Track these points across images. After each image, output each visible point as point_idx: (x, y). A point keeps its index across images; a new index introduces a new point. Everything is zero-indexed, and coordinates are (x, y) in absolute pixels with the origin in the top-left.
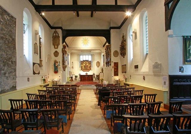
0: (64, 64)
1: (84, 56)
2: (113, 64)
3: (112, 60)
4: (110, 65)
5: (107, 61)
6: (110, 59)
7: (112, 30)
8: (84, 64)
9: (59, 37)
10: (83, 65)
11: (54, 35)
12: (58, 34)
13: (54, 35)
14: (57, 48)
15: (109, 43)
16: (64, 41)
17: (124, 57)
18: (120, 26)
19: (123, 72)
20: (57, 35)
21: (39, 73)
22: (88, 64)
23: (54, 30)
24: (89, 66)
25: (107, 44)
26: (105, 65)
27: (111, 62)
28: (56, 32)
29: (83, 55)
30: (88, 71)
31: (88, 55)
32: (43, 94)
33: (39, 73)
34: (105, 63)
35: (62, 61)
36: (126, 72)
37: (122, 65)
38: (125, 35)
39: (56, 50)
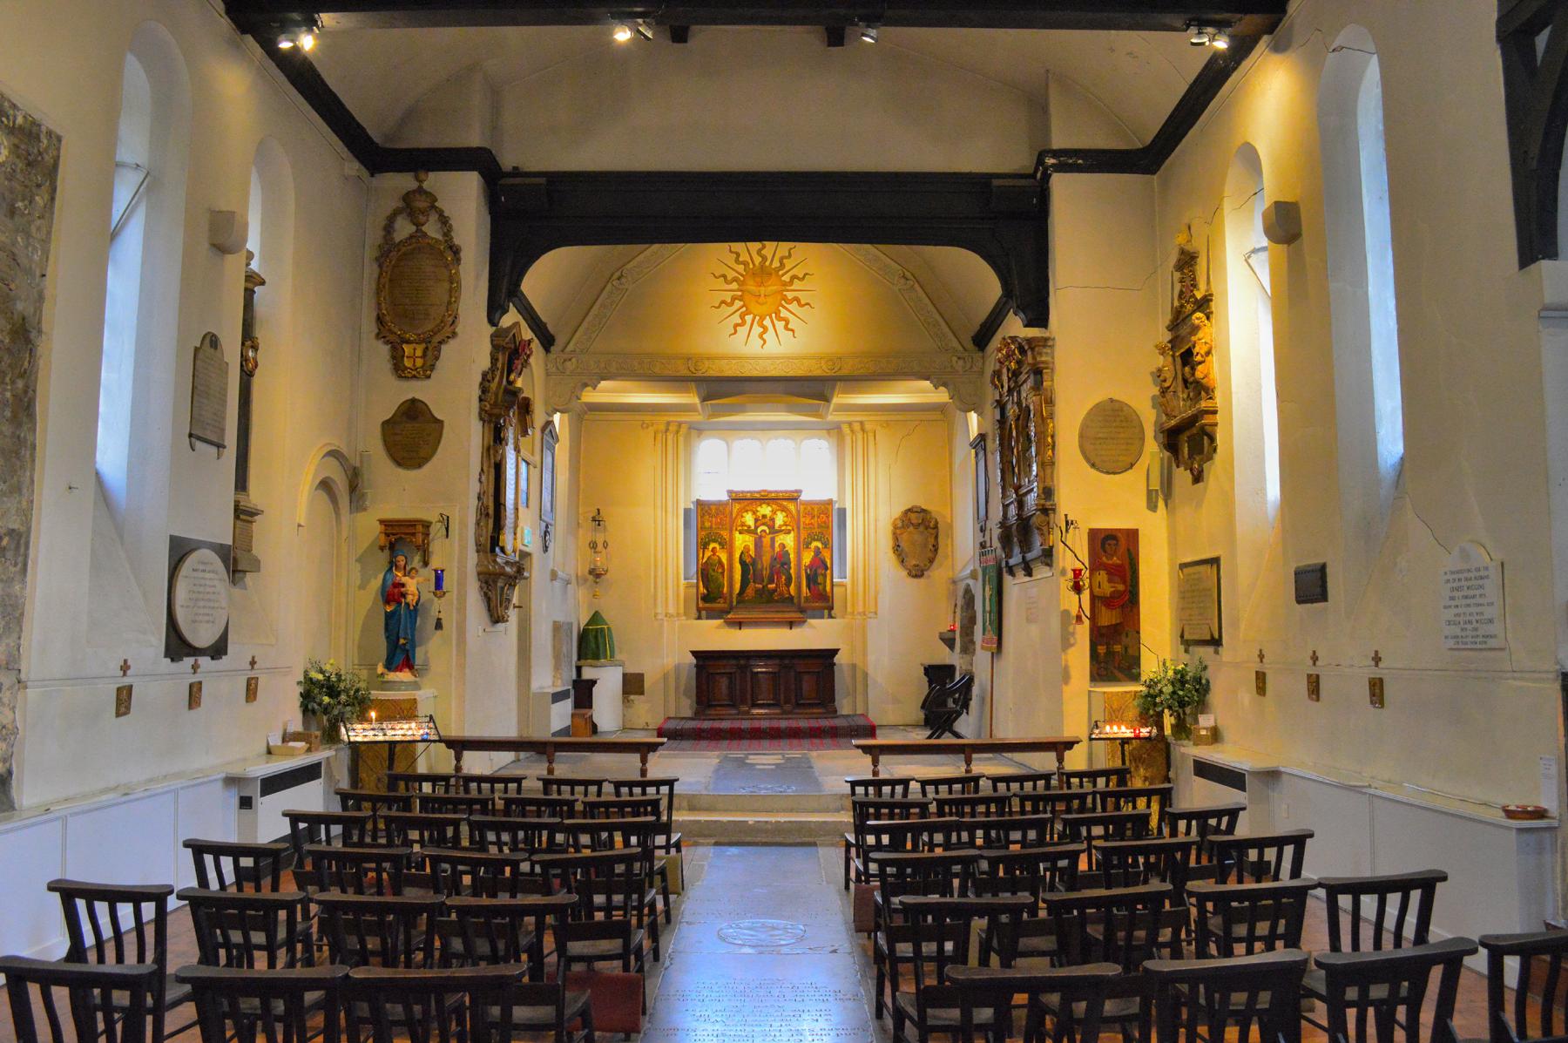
0: (495, 541)
2: (1073, 553)
3: (1068, 502)
4: (1048, 556)
5: (1013, 510)
6: (1048, 493)
7: (1064, 188)
9: (456, 251)
10: (728, 545)
11: (404, 229)
12: (444, 221)
13: (404, 229)
14: (426, 371)
15: (1038, 314)
16: (504, 291)
18: (1148, 139)
20: (432, 229)
22: (789, 541)
23: (403, 182)
24: (807, 558)
25: (1015, 326)
27: (1046, 529)
28: (416, 206)
30: (791, 624)
35: (482, 513)
37: (1183, 566)
38: (1198, 244)
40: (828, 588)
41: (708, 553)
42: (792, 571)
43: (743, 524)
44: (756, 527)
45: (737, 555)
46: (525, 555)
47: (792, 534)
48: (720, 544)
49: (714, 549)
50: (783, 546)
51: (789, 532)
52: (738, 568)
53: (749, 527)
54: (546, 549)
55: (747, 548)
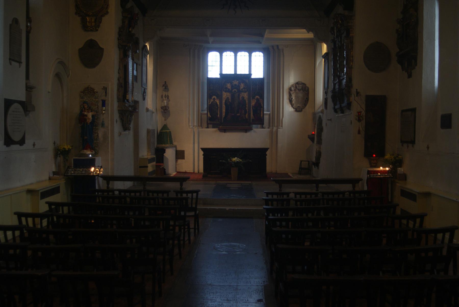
1: (228, 56)
8: (225, 95)
10: (220, 97)
17: (410, 76)
19: (403, 142)
21: (22, 142)
22: (245, 95)
24: (253, 103)
26: (330, 104)
29: (221, 51)
31: (250, 51)
32: (39, 226)
33: (22, 142)
34: (330, 94)
36: (413, 142)
37: (403, 111)
39: (94, 36)
40: (262, 115)
41: (212, 100)
42: (247, 108)
43: (226, 88)
44: (232, 89)
45: (224, 102)
46: (136, 102)
47: (247, 93)
48: (217, 96)
49: (214, 99)
50: (243, 98)
51: (245, 92)
52: (224, 106)
53: (229, 89)
54: (144, 99)
55: (228, 98)
